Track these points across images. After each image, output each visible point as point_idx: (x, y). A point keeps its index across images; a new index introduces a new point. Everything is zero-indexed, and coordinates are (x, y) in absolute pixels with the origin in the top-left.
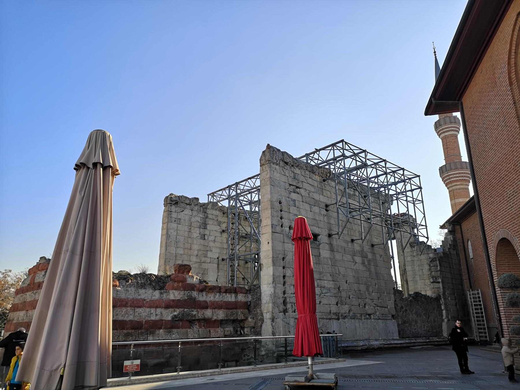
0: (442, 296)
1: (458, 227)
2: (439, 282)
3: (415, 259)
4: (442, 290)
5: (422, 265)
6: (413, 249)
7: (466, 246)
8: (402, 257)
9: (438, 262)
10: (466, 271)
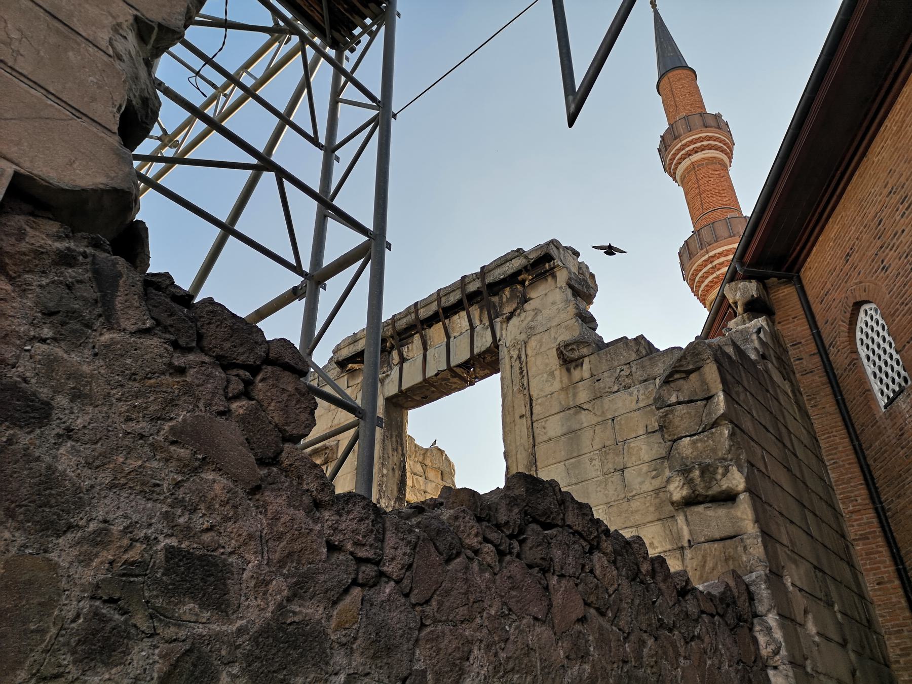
0: (763, 591)
1: (786, 295)
2: (729, 498)
3: (586, 418)
4: (757, 550)
5: (620, 445)
6: (576, 374)
7: (839, 359)
8: (522, 427)
9: (711, 372)
10: (861, 494)
